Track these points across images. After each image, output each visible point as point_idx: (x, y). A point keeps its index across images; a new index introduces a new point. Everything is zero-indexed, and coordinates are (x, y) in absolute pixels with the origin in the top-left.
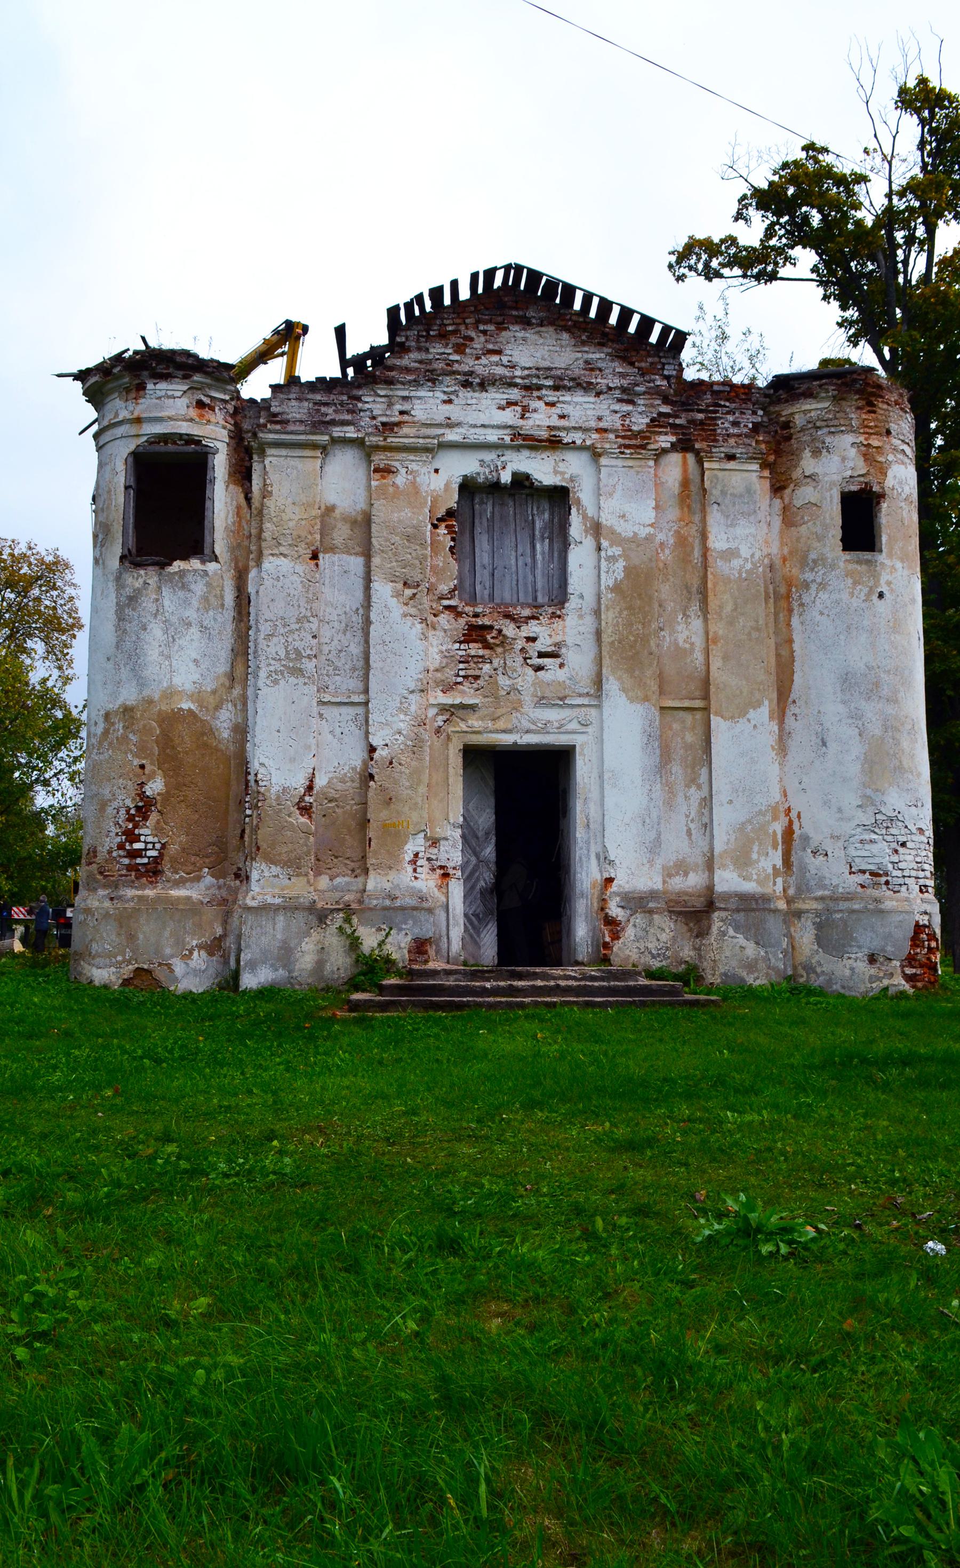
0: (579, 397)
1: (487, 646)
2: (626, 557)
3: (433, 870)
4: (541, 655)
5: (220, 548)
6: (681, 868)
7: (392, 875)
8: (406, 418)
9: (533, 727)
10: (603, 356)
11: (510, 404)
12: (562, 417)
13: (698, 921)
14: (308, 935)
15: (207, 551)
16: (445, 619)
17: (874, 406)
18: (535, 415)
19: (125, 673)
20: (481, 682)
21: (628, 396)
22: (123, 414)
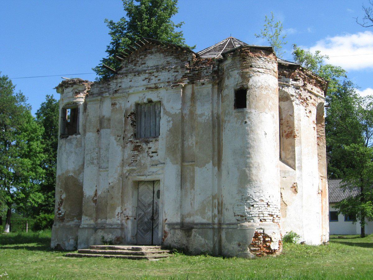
1: (139, 151)
2: (173, 120)
3: (125, 217)
4: (153, 153)
7: (113, 219)
8: (120, 88)
9: (149, 174)
10: (172, 58)
11: (146, 79)
12: (159, 80)
13: (188, 232)
14: (92, 235)
15: (77, 132)
16: (129, 145)
17: (245, 59)
18: (152, 81)
20: (137, 162)
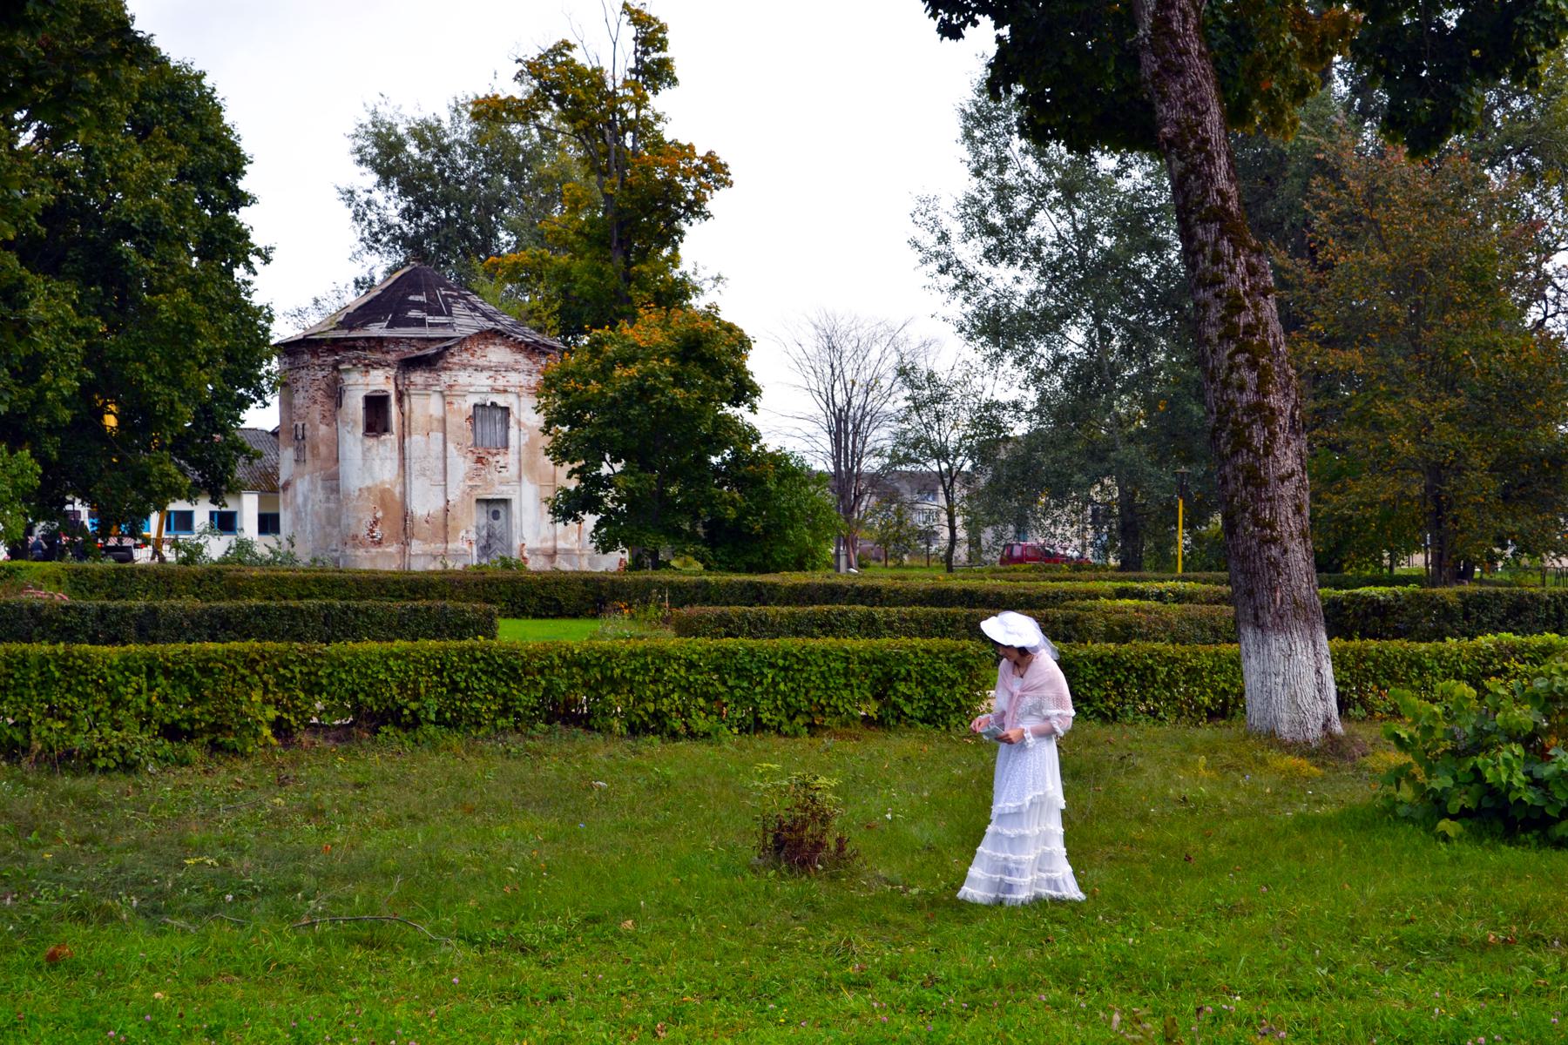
0: (513, 374)
5: (394, 430)
6: (545, 540)
16: (469, 455)
19: (367, 475)
21: (530, 373)
22: (360, 381)
